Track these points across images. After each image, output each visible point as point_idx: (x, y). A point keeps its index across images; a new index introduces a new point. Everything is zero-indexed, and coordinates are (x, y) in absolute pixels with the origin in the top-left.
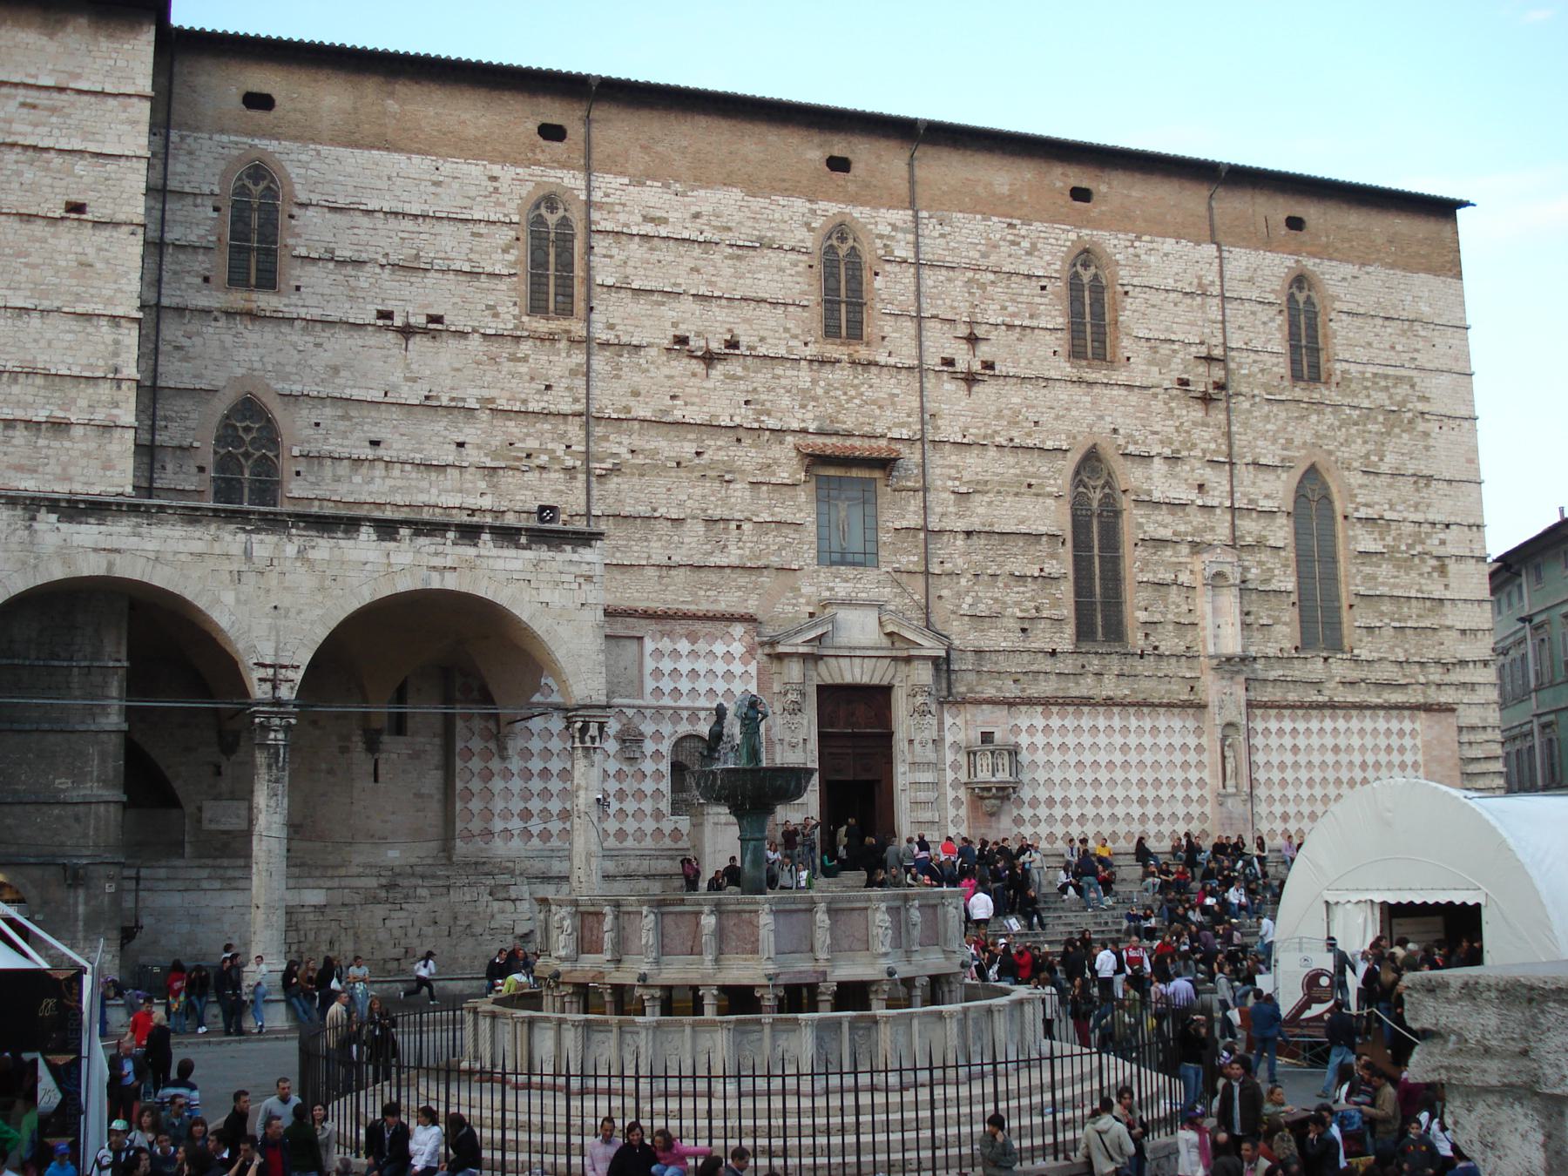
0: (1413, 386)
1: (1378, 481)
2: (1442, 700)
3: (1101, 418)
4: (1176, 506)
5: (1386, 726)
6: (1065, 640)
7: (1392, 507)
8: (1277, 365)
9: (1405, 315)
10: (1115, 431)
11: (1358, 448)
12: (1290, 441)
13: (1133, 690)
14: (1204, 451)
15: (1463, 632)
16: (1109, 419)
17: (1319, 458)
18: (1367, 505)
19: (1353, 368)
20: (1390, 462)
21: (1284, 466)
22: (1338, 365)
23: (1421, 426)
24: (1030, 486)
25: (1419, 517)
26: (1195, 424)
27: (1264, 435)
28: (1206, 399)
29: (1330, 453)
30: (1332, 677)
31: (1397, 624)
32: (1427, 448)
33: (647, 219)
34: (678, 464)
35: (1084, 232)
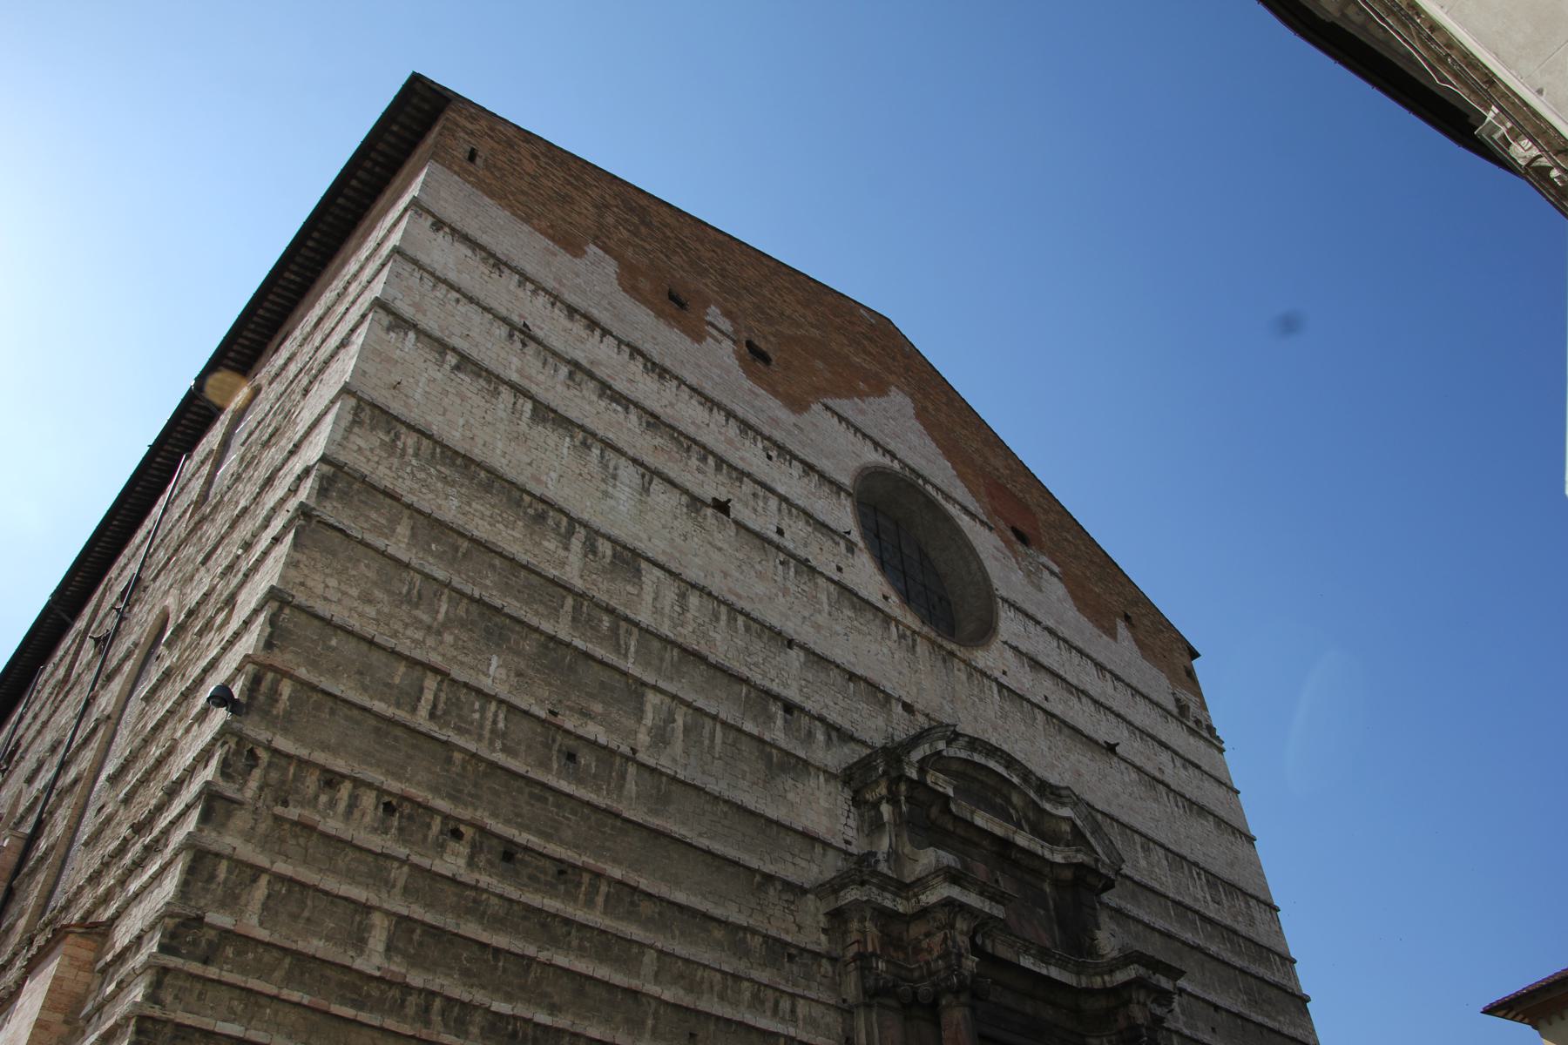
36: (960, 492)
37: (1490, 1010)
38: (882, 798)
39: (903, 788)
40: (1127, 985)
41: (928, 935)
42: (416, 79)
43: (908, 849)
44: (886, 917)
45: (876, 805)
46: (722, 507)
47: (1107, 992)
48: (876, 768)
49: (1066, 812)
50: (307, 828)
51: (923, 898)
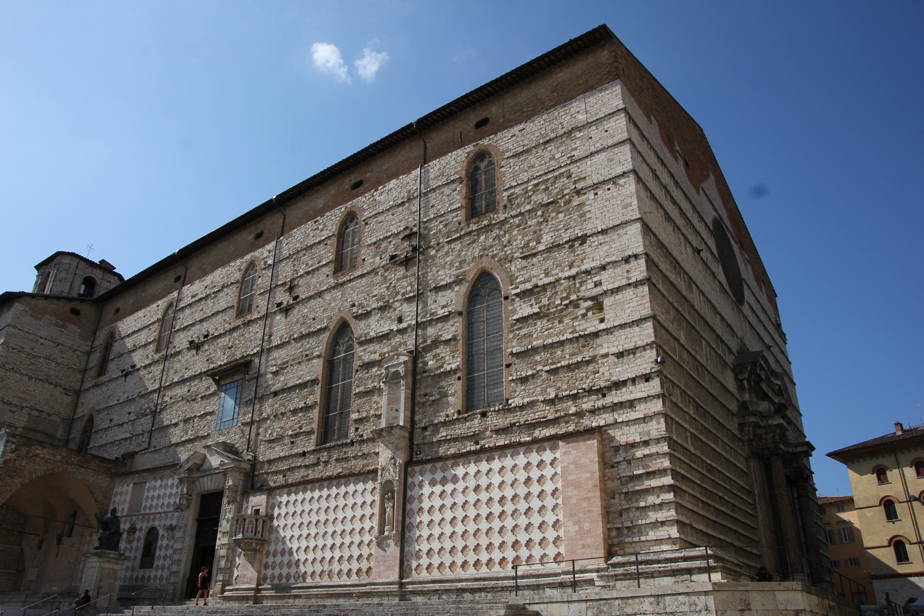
0: (569, 177)
1: (535, 260)
2: (594, 424)
3: (347, 300)
4: (386, 336)
5: (525, 461)
6: (310, 444)
7: (547, 274)
8: (457, 216)
9: (561, 132)
10: (353, 305)
11: (519, 241)
12: (462, 262)
13: (343, 468)
14: (403, 294)
15: (620, 355)
16: (349, 300)
17: (486, 263)
18: (524, 282)
19: (518, 190)
20: (547, 239)
21: (458, 281)
22: (505, 194)
23: (576, 201)
24: (307, 356)
25: (573, 272)
26: (398, 280)
27: (443, 267)
28: (407, 262)
29: (496, 255)
30: (486, 429)
31: (547, 368)
32: (583, 215)
33: (193, 297)
34: (183, 399)
35: (349, 204)
36: (729, 225)
37: (829, 455)
38: (744, 379)
39: (753, 376)
40: (801, 452)
41: (765, 433)
42: (604, 27)
43: (754, 400)
44: (757, 426)
45: (742, 381)
46: (699, 252)
47: (793, 454)
48: (747, 368)
49: (778, 382)
50: (675, 404)
51: (770, 422)
